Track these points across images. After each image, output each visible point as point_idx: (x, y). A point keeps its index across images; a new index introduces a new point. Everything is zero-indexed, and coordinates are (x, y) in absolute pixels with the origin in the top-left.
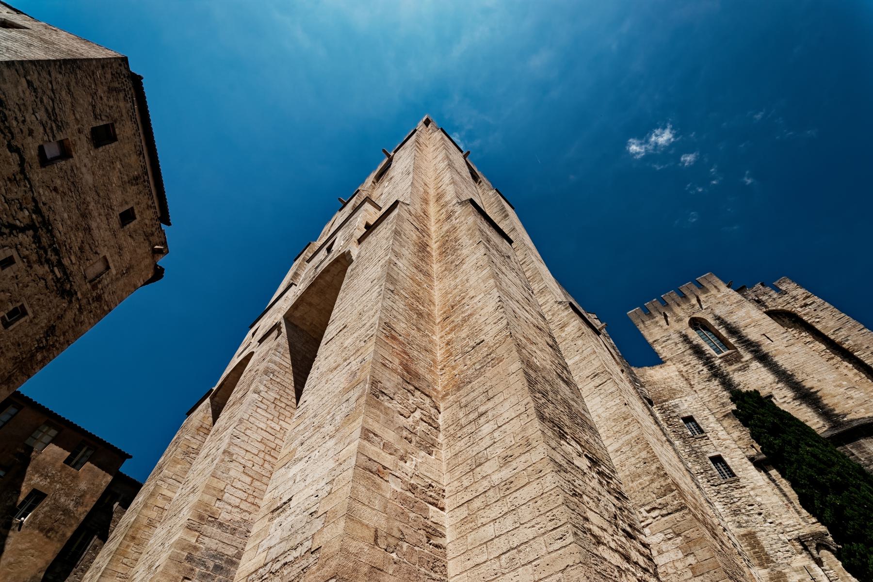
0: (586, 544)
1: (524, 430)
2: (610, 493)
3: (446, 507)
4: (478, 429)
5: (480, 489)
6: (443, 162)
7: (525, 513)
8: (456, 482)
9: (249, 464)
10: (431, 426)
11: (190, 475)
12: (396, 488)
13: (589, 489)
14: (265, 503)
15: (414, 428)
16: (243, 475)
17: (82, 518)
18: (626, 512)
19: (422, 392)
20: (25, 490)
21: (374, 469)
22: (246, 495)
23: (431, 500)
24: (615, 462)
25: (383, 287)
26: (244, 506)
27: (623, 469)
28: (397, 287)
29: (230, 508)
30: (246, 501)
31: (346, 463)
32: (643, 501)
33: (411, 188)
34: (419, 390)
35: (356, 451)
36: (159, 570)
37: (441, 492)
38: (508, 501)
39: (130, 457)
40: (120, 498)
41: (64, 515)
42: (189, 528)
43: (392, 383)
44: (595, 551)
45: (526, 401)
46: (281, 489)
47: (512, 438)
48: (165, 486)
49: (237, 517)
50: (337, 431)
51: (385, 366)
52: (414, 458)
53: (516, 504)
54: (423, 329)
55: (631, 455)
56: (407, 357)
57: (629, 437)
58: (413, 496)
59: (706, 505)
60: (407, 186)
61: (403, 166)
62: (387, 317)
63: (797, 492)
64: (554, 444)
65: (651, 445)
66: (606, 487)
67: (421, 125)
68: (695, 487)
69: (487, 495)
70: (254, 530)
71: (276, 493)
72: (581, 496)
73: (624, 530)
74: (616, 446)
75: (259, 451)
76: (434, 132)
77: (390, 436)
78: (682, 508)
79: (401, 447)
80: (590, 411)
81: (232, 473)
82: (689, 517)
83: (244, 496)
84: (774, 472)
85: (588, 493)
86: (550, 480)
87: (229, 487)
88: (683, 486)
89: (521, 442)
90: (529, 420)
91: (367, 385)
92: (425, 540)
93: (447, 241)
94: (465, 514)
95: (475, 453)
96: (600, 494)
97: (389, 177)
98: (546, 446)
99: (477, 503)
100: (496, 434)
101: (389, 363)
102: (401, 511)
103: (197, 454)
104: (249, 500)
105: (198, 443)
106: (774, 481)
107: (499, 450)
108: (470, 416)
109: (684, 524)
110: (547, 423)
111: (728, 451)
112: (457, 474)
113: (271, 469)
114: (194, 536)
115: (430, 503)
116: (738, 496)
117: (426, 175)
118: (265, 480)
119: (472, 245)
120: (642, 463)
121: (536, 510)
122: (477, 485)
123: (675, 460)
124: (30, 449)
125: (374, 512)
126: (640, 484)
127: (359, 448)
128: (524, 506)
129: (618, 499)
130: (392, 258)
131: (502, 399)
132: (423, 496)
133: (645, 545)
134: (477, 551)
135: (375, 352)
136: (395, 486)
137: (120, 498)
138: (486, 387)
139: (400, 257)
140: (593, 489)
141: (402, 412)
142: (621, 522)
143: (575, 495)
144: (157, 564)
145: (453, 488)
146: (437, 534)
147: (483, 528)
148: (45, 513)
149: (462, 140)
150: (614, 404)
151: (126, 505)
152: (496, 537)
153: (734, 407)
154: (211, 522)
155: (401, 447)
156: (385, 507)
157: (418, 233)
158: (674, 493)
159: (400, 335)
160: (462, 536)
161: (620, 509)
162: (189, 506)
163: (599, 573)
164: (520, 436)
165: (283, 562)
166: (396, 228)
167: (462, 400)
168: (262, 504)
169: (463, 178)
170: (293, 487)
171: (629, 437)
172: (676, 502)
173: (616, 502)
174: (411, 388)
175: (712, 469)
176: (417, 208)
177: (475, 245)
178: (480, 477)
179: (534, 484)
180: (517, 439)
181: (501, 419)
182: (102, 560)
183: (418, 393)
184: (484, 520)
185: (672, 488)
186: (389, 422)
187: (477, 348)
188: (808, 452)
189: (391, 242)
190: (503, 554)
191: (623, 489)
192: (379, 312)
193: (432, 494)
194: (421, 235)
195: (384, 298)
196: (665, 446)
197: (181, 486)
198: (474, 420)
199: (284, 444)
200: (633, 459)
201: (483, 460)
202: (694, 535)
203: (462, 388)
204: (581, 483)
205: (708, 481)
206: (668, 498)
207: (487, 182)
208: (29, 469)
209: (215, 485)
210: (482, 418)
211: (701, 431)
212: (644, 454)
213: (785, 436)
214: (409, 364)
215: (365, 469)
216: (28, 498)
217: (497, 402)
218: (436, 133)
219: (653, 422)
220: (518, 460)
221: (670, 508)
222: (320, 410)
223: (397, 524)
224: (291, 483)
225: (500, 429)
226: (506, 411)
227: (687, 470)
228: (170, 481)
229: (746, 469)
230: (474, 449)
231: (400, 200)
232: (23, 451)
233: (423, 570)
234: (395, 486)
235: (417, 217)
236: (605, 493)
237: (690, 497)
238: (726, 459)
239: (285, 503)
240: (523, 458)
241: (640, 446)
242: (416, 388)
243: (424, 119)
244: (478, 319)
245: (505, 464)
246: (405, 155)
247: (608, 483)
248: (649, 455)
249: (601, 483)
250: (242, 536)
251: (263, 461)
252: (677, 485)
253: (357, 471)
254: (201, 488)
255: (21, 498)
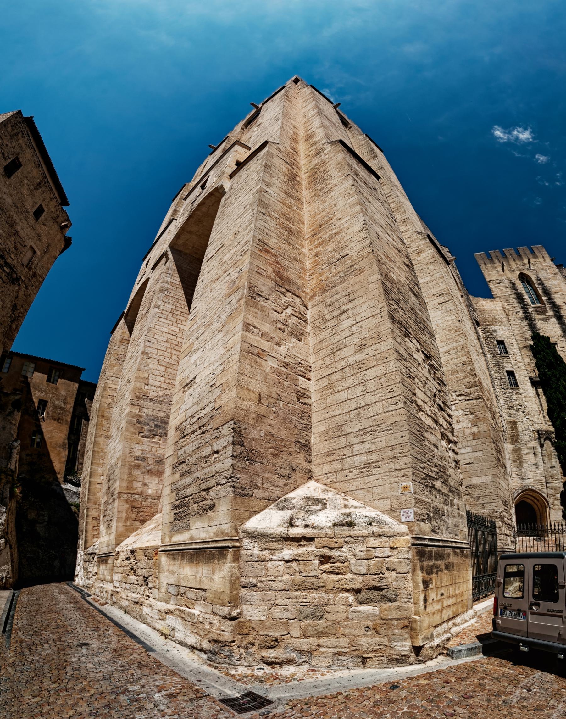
0: (411, 410)
1: (377, 327)
2: (434, 379)
3: (312, 378)
4: (340, 323)
5: (338, 367)
6: (313, 110)
7: (371, 386)
8: (320, 361)
9: (161, 358)
10: (301, 319)
11: (124, 372)
12: (273, 365)
13: (421, 375)
14: (178, 381)
15: (287, 321)
16: (159, 366)
17: (71, 410)
18: (443, 393)
19: (293, 294)
20: (36, 401)
21: (256, 352)
22: (164, 379)
23: (300, 373)
24: (443, 359)
25: (255, 211)
26: (164, 386)
27: (448, 365)
28: (268, 210)
29: (155, 388)
30: (164, 382)
31: (233, 349)
32: (456, 388)
33: (280, 130)
34: (290, 292)
35: (240, 340)
36: (124, 429)
37: (308, 368)
38: (360, 376)
39: (84, 369)
40: (87, 395)
41: (61, 410)
42: (133, 404)
43: (267, 287)
44: (416, 415)
45: (381, 306)
46: (187, 372)
47: (367, 332)
48: (110, 382)
49: (161, 393)
50: (223, 326)
51: (260, 274)
52: (287, 344)
53: (365, 379)
54: (293, 243)
55: (455, 357)
56: (279, 266)
57: (456, 344)
58: (286, 370)
59: (495, 399)
60: (276, 129)
61: (271, 114)
62: (260, 234)
63: (548, 406)
64: (399, 340)
65: (471, 353)
66: (433, 375)
67: (289, 83)
68: (491, 387)
69: (344, 371)
70: (174, 400)
71: (184, 375)
72: (414, 379)
73: (438, 405)
74: (446, 349)
75: (167, 348)
76: (303, 87)
77: (267, 327)
78: (480, 398)
79: (276, 335)
80: (432, 320)
81: (151, 366)
82: (482, 404)
83: (162, 379)
84: (540, 391)
85: (419, 377)
86: (393, 365)
87: (151, 375)
88: (484, 384)
89: (374, 336)
90: (382, 320)
91: (245, 290)
92: (296, 399)
93: (316, 172)
94: (326, 383)
95: (336, 341)
96: (427, 379)
97: (258, 124)
98: (393, 341)
99: (336, 377)
100: (354, 328)
101: (263, 272)
102: (277, 381)
103: (125, 358)
104: (166, 382)
105: (123, 350)
106: (538, 395)
107: (356, 340)
108: (333, 313)
109: (477, 408)
110: (396, 324)
111: (519, 369)
112: (321, 355)
113: (178, 359)
114: (137, 409)
115: (300, 375)
116: (515, 398)
117: (295, 120)
118: (174, 367)
119: (341, 176)
120: (461, 364)
121: (379, 384)
122: (336, 364)
123: (484, 367)
124: (26, 378)
125: (258, 382)
126: (457, 377)
127: (242, 337)
128: (371, 381)
129: (439, 384)
130: (263, 187)
131: (361, 302)
132: (295, 370)
133: (450, 416)
134: (334, 408)
135: (251, 263)
136: (272, 363)
137: (87, 395)
138: (348, 291)
139: (271, 186)
140: (423, 375)
141: (276, 309)
142: (438, 399)
143: (409, 377)
144: (121, 427)
145: (318, 366)
146: (305, 396)
147: (339, 393)
148: (51, 411)
149: (332, 94)
150: (451, 319)
151: (91, 398)
152: (348, 400)
153: (532, 343)
154: (145, 399)
155: (276, 335)
156: (266, 378)
157: (287, 166)
158: (477, 387)
159: (273, 249)
160: (323, 398)
161: (439, 391)
162: (129, 391)
163: (417, 424)
164: (374, 331)
165: (197, 417)
166: (266, 163)
167: (328, 301)
168: (176, 383)
169: (334, 124)
170: (196, 370)
171: (456, 344)
172: (477, 394)
173: (437, 386)
174: (283, 290)
175: (505, 378)
176: (287, 146)
177: (344, 177)
178: (339, 358)
179: (381, 367)
180: (371, 333)
181: (360, 317)
182: (91, 429)
183: (289, 294)
184: (340, 388)
185: (477, 384)
186: (265, 317)
187: (342, 260)
188: (563, 385)
189: (261, 174)
190: (352, 410)
191: (444, 378)
192: (252, 231)
193: (301, 369)
194: (290, 168)
195: (256, 220)
196: (480, 356)
197: (120, 380)
198: (337, 316)
199: (184, 340)
200: (456, 360)
201: (342, 346)
202: (481, 415)
203: (328, 291)
204: (415, 370)
205: (501, 385)
206: (473, 390)
207: (357, 128)
208: (31, 389)
209: (141, 375)
210: (343, 315)
211: (507, 352)
212: (464, 359)
213: (554, 371)
214: (281, 271)
215: (248, 352)
216: (39, 404)
217: (357, 304)
218: (306, 89)
219: (476, 338)
220: (370, 348)
221: (472, 396)
222: (208, 313)
223: (275, 389)
224: (194, 367)
225: (357, 325)
226: (364, 311)
227: (490, 375)
228: (112, 378)
229: (526, 384)
230: (336, 338)
231: (269, 140)
232: (23, 379)
233: (294, 418)
234: (272, 363)
235: (287, 154)
236: (431, 379)
237: (486, 392)
238: (516, 375)
239: (192, 381)
240: (374, 347)
241: (463, 352)
242: (288, 291)
243: (293, 79)
244: (345, 237)
245: (359, 351)
246: (274, 106)
247: (435, 373)
248: (468, 360)
249: (429, 372)
250: (167, 405)
251: (170, 355)
252: (481, 383)
253: (242, 354)
254: (133, 379)
255: (36, 405)
